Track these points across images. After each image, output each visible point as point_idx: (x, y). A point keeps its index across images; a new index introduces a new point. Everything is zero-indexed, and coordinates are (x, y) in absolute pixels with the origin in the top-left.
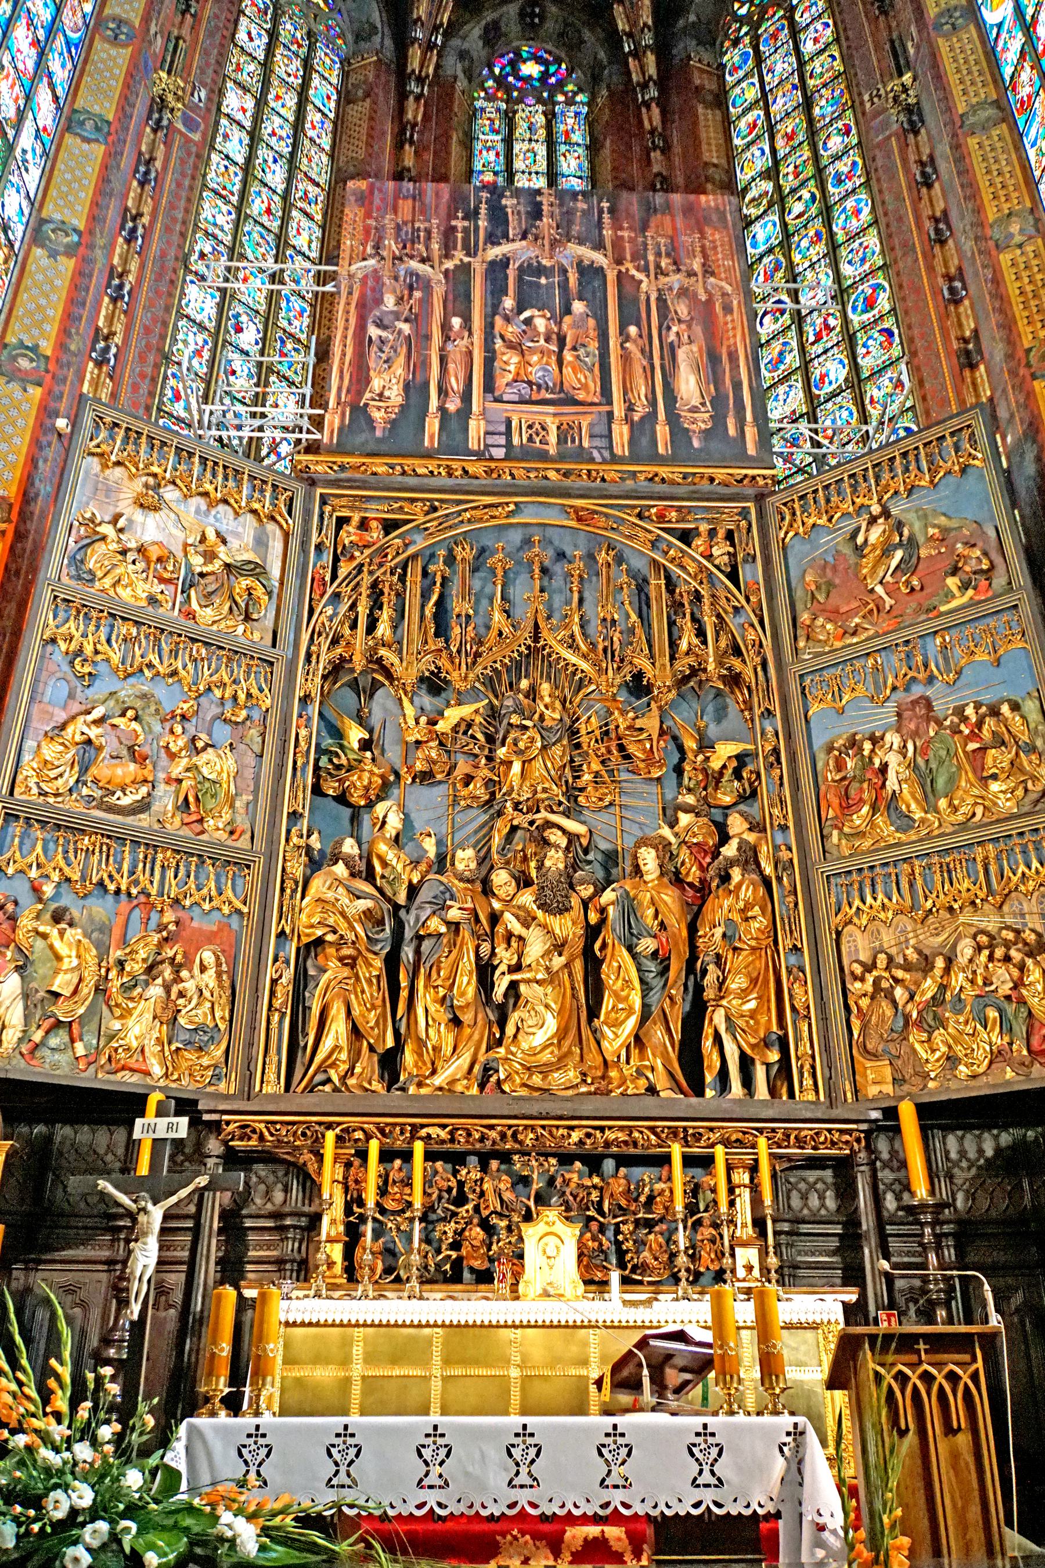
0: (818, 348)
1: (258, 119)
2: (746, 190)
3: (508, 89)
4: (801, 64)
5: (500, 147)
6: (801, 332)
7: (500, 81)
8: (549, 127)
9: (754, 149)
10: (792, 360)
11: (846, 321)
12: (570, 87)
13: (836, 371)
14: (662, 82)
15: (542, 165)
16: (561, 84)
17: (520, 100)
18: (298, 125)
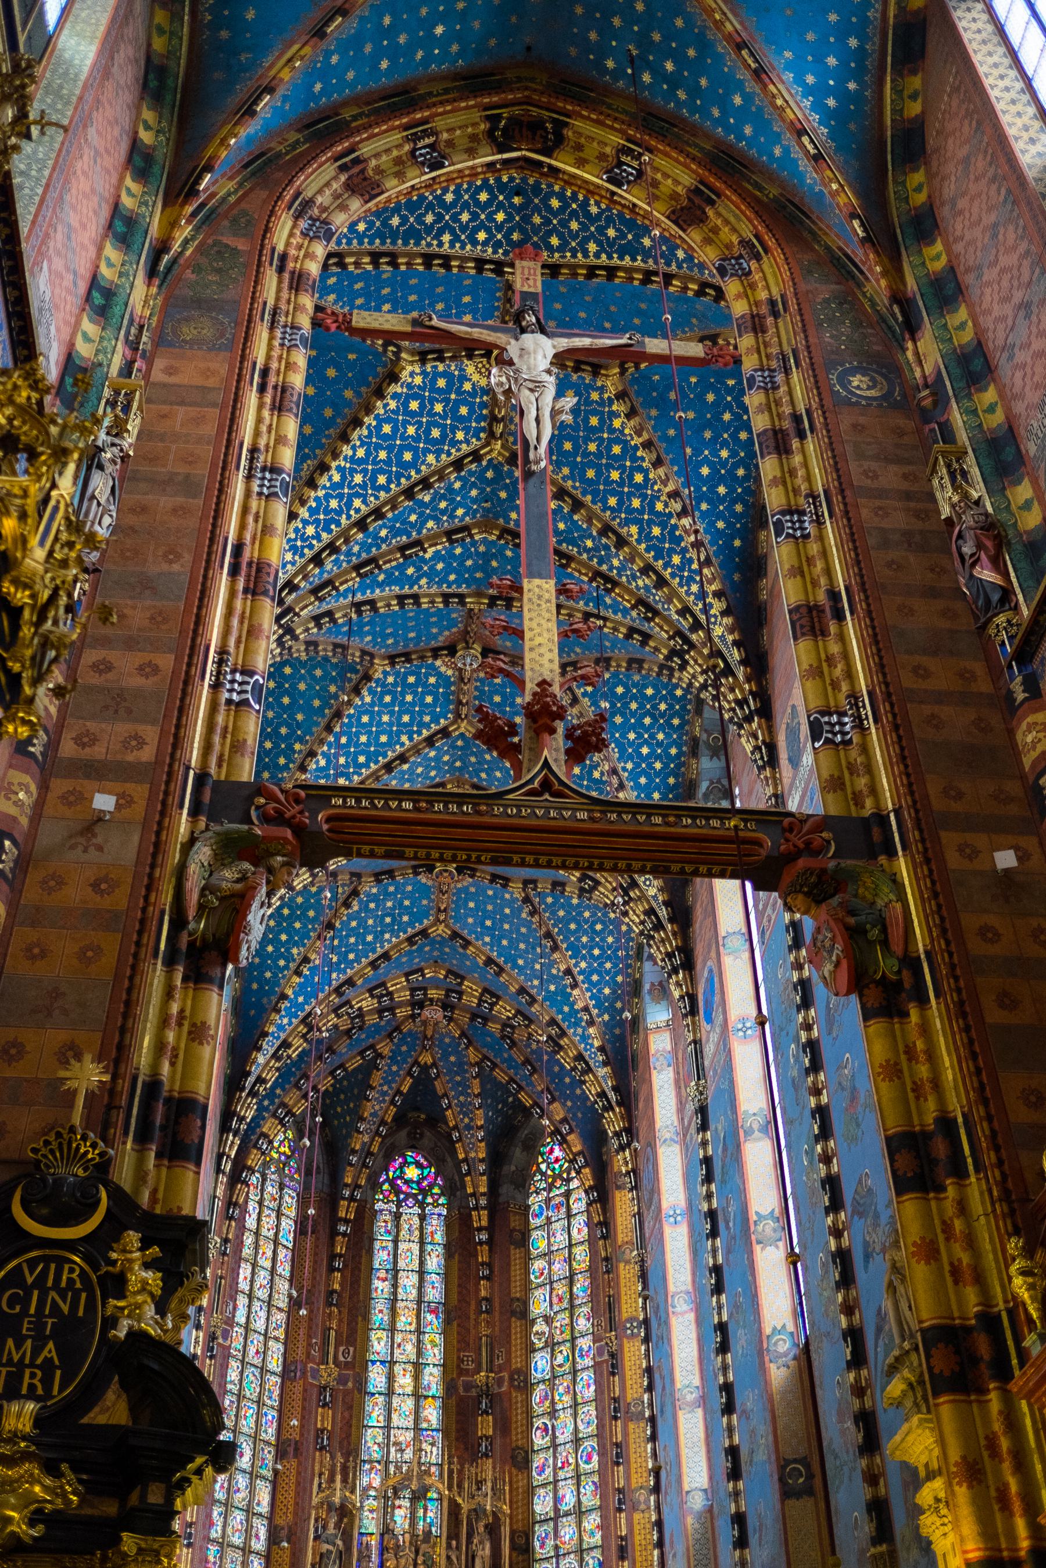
0: (561, 1474)
1: (252, 1281)
2: (533, 1322)
3: (397, 1191)
4: (570, 1246)
5: (390, 1245)
6: (555, 1458)
7: (392, 1183)
8: (421, 1229)
9: (540, 1291)
10: (549, 1471)
11: (577, 1465)
12: (436, 1190)
13: (569, 1501)
14: (490, 1229)
15: (416, 1267)
16: (431, 1186)
17: (405, 1200)
18: (273, 1271)
